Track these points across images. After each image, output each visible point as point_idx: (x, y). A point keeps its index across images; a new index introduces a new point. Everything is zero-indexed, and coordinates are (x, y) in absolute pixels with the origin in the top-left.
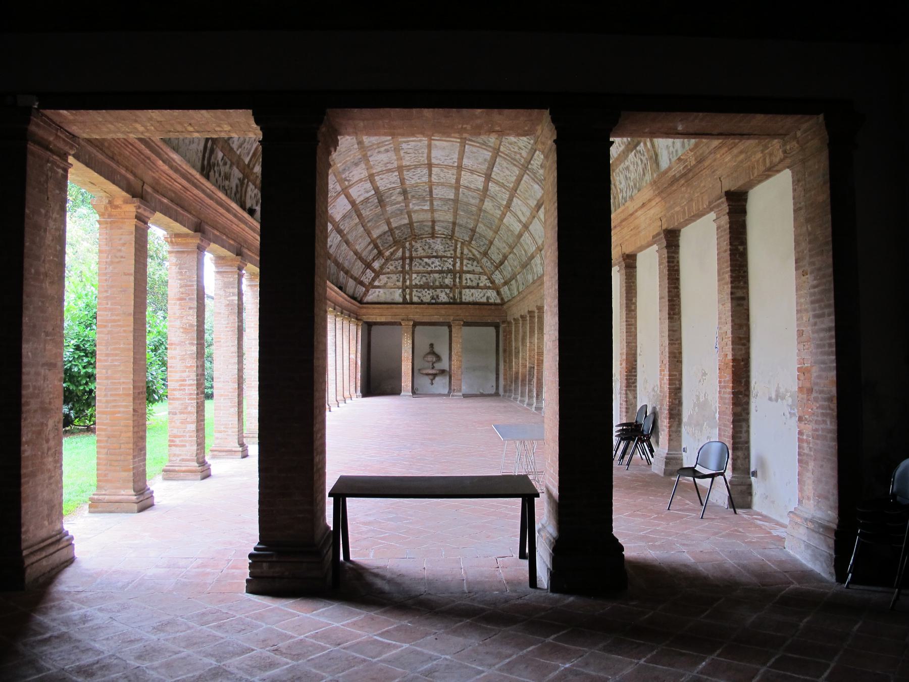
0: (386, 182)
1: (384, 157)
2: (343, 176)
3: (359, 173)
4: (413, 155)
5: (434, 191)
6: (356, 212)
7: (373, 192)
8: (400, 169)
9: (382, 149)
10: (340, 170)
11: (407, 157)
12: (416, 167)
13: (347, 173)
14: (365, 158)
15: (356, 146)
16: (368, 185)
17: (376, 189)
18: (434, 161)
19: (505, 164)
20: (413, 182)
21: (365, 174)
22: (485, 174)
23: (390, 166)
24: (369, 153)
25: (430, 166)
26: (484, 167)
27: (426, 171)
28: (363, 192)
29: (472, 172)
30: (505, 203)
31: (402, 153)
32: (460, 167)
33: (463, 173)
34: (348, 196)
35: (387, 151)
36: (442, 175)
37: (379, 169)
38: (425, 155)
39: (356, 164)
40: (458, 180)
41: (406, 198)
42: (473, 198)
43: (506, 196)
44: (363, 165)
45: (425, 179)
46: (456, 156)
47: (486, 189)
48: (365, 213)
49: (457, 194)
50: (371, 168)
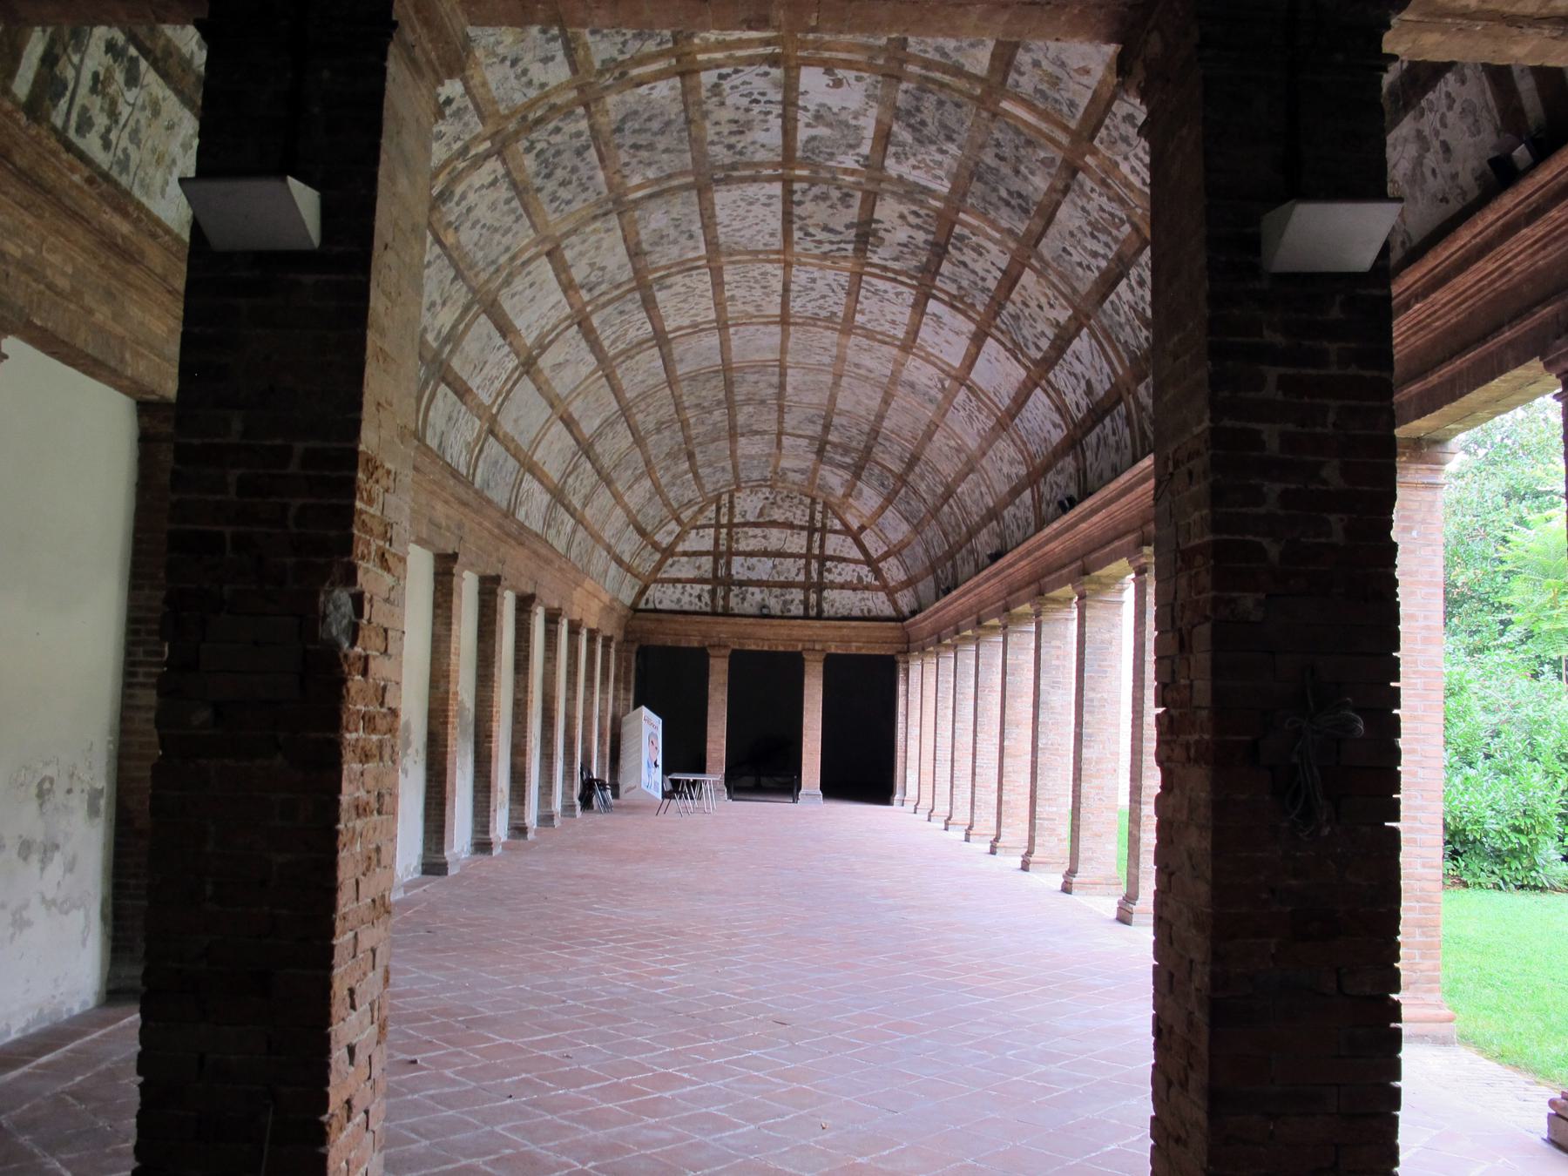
0: (888, 306)
1: (867, 360)
2: (940, 396)
3: (920, 373)
4: (815, 344)
5: (777, 224)
6: (1002, 307)
7: (933, 306)
8: (847, 327)
9: (862, 372)
10: (933, 407)
11: (827, 342)
12: (814, 320)
13: (933, 392)
14: (894, 378)
15: (893, 404)
16: (926, 333)
17: (919, 307)
18: (777, 329)
19: (651, 382)
20: (830, 274)
21: (912, 362)
22: (669, 341)
23: (865, 342)
24: (886, 380)
25: (785, 320)
26: (677, 350)
27: (796, 306)
28: (945, 333)
29: (696, 329)
30: (595, 321)
31: (834, 351)
32: (722, 325)
33: (713, 316)
34: (970, 361)
35: (857, 366)
36: (758, 292)
37: (885, 348)
38: (792, 340)
39: (912, 386)
40: (718, 284)
41: (870, 200)
42: (660, 238)
43: (606, 337)
44: (905, 375)
45: (800, 277)
46: (735, 342)
47: (649, 305)
48: (991, 261)
49: (708, 221)
50: (895, 361)
